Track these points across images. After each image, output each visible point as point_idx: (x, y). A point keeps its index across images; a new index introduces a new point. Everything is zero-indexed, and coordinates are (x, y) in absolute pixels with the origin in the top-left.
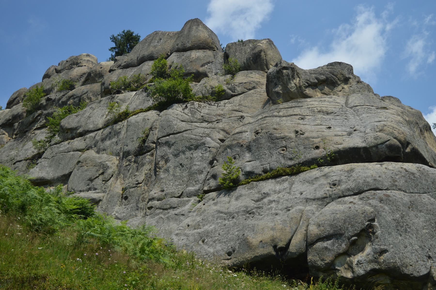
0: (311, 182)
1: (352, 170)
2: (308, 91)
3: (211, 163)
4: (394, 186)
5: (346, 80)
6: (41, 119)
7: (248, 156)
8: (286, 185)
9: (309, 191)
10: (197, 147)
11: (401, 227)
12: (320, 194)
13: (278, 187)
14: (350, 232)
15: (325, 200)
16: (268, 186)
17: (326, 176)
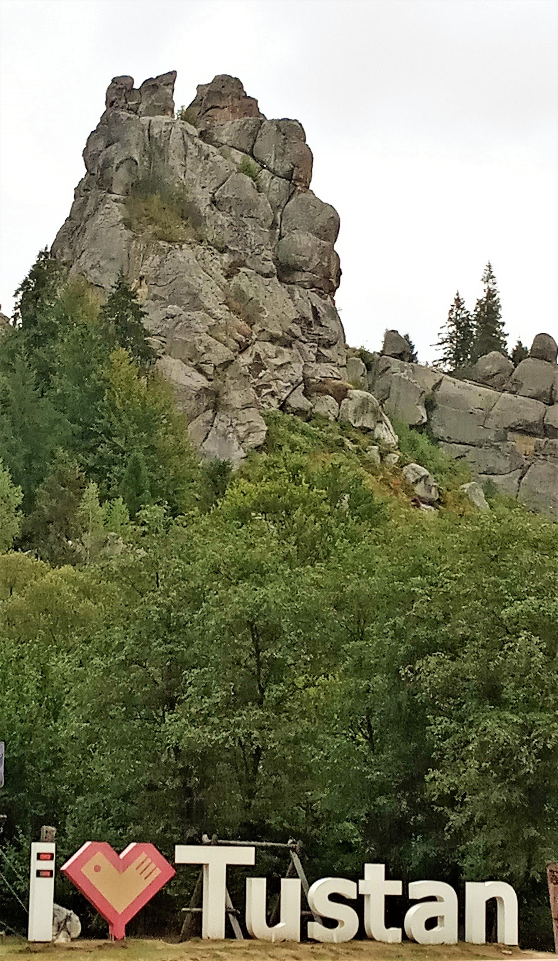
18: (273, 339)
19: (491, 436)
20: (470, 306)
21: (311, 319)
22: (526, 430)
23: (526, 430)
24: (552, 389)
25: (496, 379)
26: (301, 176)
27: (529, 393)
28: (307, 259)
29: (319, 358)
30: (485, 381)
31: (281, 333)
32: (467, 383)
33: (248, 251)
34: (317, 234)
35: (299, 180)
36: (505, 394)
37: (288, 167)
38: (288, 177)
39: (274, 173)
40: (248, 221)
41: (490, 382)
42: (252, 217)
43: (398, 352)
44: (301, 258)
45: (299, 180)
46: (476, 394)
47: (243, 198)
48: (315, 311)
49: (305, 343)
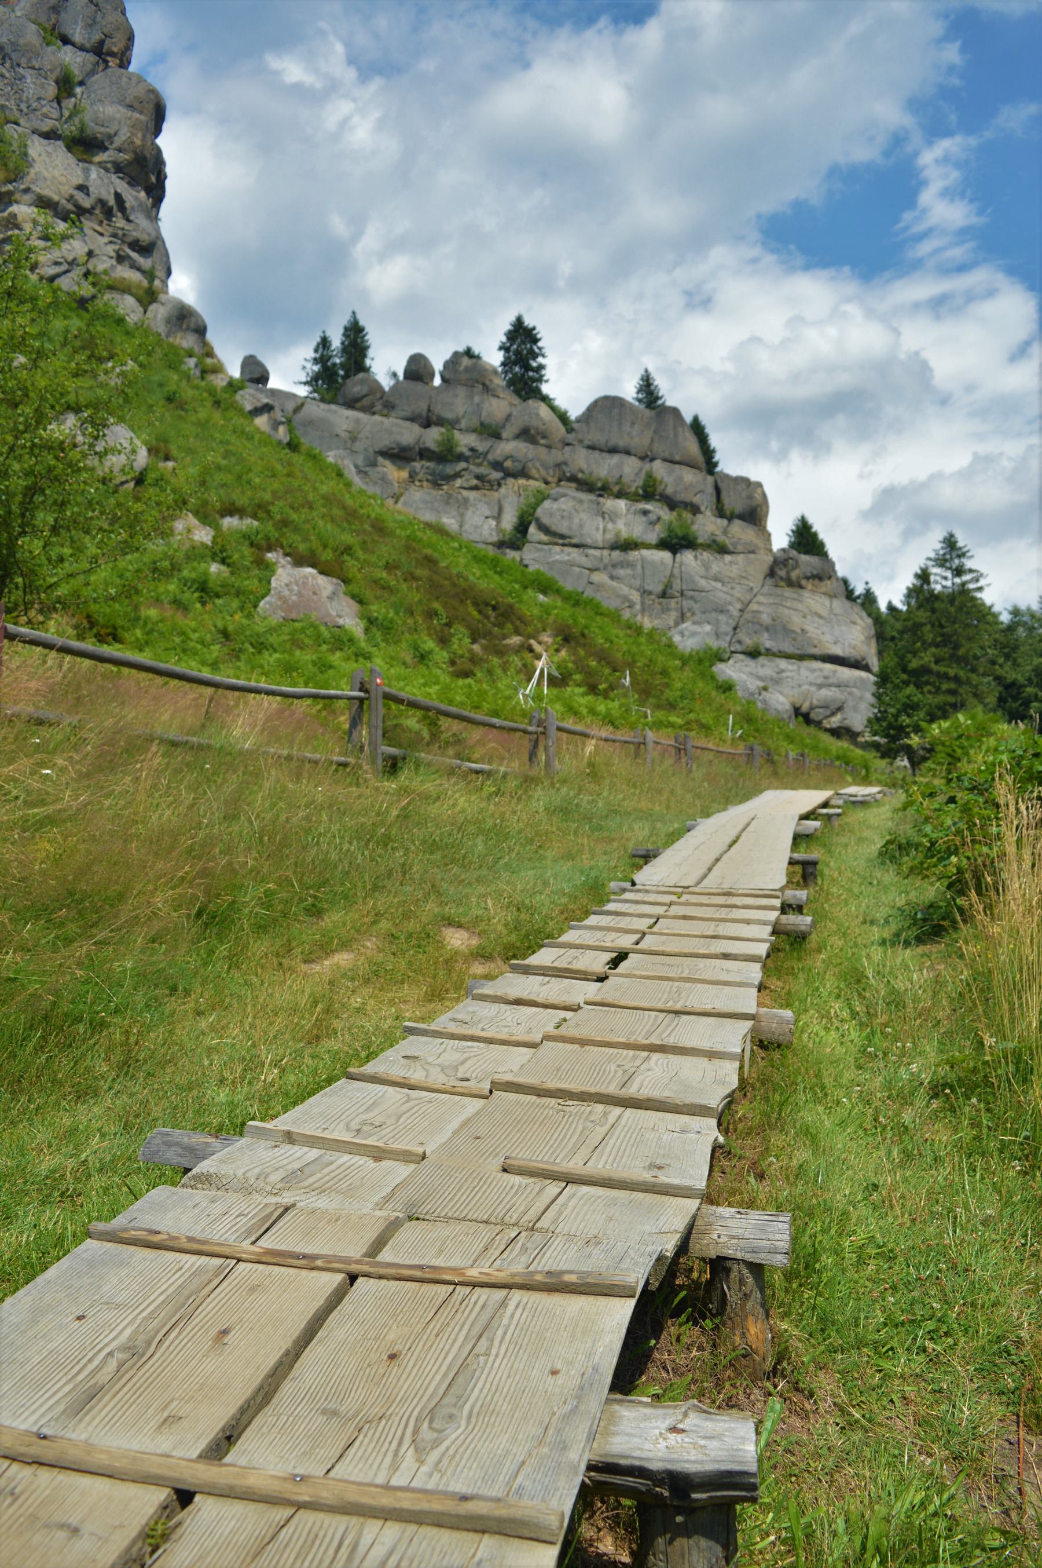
0: (813, 671)
1: (835, 672)
2: (804, 582)
3: (735, 629)
4: (855, 686)
5: (830, 578)
6: (467, 476)
7: (766, 635)
8: (795, 667)
9: (812, 677)
10: (721, 611)
11: (855, 709)
12: (819, 681)
13: (790, 667)
14: (833, 707)
15: (820, 686)
16: (783, 664)
17: (821, 670)
18: (43, 203)
19: (360, 462)
20: (336, 342)
21: (112, 202)
22: (399, 455)
23: (399, 455)
24: (429, 410)
25: (365, 402)
26: (115, 49)
27: (403, 414)
28: (112, 132)
29: (120, 259)
30: (351, 404)
31: (56, 198)
32: (333, 407)
33: (23, 106)
34: (130, 106)
35: (113, 54)
36: (377, 418)
37: (97, 36)
38: (99, 51)
39: (82, 48)
40: (28, 74)
41: (358, 405)
42: (33, 68)
43: (256, 376)
44: (102, 129)
45: (113, 54)
46: (343, 418)
47: (21, 41)
48: (118, 196)
49: (101, 234)
